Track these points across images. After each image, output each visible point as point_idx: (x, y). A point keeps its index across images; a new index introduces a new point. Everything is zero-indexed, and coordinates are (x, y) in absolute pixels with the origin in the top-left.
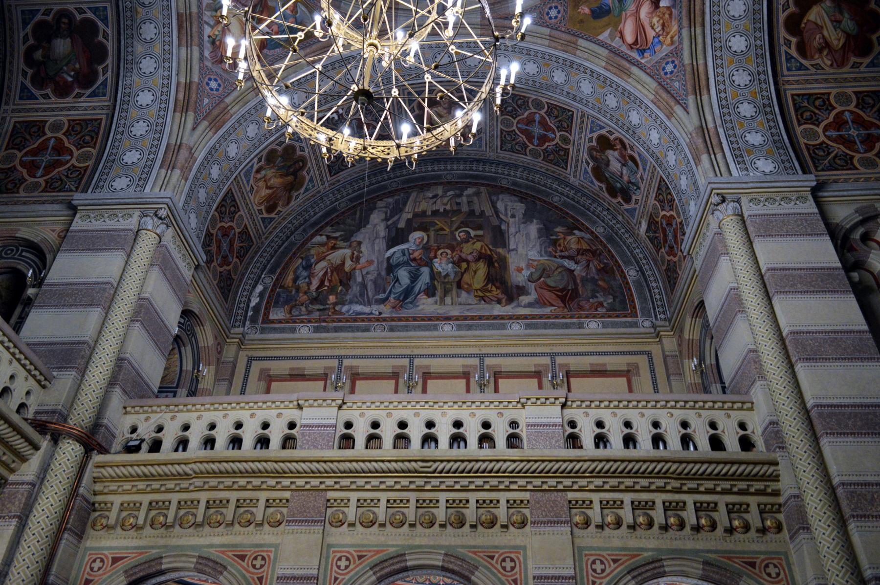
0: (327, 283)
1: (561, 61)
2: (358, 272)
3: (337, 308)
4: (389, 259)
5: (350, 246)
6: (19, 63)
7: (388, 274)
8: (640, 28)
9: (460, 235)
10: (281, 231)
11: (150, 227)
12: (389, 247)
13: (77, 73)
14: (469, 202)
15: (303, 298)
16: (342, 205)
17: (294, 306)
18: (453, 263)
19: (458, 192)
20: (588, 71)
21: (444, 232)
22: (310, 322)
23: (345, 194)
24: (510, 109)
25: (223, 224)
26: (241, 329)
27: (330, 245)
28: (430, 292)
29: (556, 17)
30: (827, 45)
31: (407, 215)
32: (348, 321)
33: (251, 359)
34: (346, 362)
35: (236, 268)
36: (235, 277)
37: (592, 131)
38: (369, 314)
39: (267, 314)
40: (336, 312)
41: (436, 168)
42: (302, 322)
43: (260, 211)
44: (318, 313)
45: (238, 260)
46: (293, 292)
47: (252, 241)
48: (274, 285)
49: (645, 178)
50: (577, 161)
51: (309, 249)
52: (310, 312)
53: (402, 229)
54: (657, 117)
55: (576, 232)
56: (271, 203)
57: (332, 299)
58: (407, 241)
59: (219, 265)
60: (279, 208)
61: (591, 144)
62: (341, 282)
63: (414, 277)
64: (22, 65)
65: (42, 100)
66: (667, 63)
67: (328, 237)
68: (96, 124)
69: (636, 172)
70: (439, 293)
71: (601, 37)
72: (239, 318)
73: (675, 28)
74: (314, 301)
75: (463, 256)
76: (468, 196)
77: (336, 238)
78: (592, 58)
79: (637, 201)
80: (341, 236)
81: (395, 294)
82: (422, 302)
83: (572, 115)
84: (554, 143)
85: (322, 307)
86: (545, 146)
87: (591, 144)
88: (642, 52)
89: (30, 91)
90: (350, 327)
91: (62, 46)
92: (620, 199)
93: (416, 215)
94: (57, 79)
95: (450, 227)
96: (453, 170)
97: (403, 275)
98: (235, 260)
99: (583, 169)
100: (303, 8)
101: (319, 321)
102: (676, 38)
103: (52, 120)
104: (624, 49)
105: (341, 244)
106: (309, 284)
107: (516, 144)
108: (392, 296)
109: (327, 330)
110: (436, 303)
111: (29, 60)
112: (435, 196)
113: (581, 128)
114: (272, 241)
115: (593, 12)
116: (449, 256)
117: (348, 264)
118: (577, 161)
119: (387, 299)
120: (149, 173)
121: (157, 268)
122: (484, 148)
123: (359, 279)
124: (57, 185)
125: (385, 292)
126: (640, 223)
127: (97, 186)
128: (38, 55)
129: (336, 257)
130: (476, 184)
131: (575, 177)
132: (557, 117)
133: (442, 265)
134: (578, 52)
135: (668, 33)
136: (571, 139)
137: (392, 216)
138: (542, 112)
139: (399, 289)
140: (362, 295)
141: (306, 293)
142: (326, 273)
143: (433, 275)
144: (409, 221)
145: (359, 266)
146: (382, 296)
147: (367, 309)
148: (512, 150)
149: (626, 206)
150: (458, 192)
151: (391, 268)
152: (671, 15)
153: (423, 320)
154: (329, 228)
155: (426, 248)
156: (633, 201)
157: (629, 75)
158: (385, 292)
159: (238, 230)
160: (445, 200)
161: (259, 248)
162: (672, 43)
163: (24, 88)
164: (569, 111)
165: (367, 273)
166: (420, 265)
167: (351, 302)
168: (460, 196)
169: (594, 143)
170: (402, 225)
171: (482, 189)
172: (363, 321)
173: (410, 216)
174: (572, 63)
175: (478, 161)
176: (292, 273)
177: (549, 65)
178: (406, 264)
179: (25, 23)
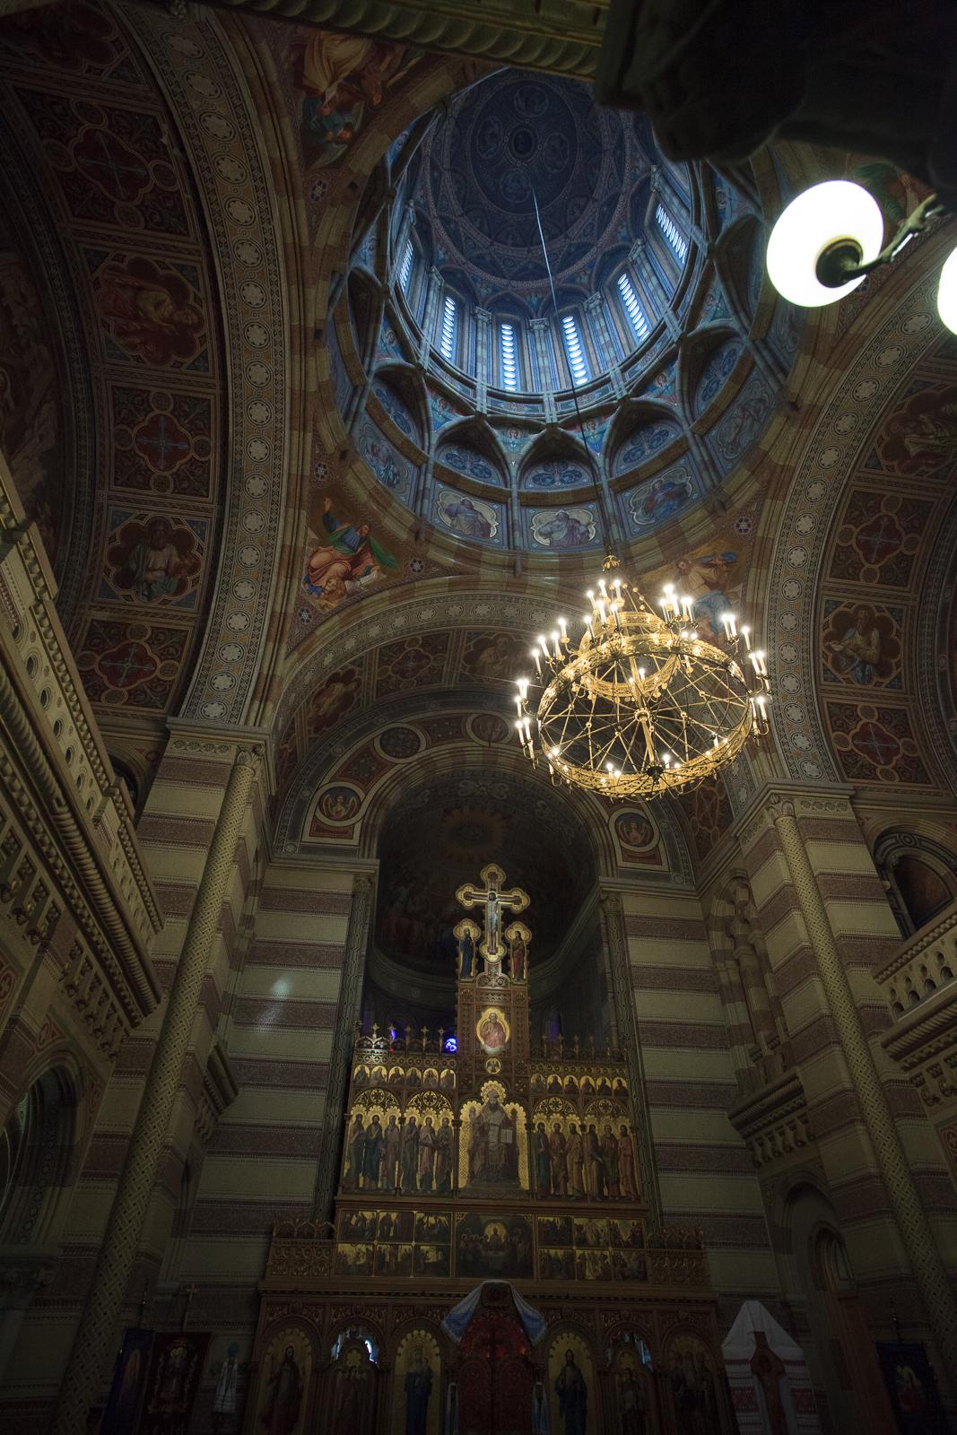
8: (325, 567)
20: (274, 524)
24: (186, 408)
30: (319, 707)
37: (191, 523)
49: (168, 607)
50: (137, 502)
54: (262, 621)
55: (52, 529)
61: (172, 522)
66: (307, 611)
69: (168, 592)
71: (310, 532)
73: (334, 605)
78: (289, 528)
79: (127, 597)
83: (202, 495)
84: (153, 469)
86: (142, 455)
87: (172, 522)
88: (308, 581)
92: (114, 571)
99: (128, 510)
100: (339, 154)
102: (328, 610)
104: (306, 559)
113: (188, 507)
115: (327, 515)
118: (137, 502)
126: (102, 609)
131: (110, 498)
132: (192, 473)
135: (327, 599)
136: (168, 493)
138: (192, 453)
149: (110, 581)
152: (342, 595)
156: (126, 592)
157: (290, 577)
162: (323, 608)
164: (207, 491)
169: (175, 527)
174: (278, 503)
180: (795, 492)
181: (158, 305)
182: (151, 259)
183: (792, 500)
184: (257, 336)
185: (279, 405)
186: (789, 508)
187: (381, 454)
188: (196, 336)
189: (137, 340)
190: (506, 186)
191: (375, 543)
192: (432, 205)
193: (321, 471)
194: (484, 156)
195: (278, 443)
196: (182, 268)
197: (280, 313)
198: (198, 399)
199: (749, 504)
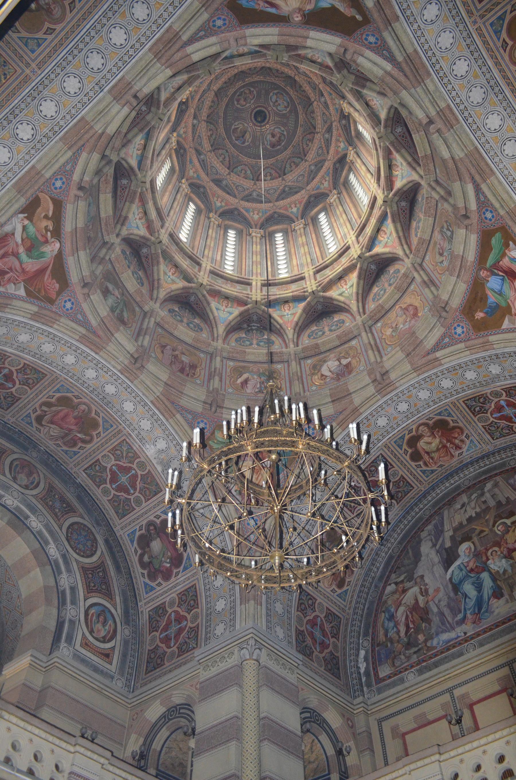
0: (411, 626)
1: (487, 359)
2: (431, 603)
3: (429, 644)
4: (451, 579)
5: (416, 583)
6: (138, 570)
7: (456, 594)
9: (499, 529)
10: (358, 596)
11: (248, 657)
12: (446, 569)
13: (171, 559)
14: (492, 496)
15: (398, 647)
16: (395, 551)
17: (395, 658)
18: (505, 557)
19: (479, 492)
21: (485, 533)
22: (412, 667)
23: (393, 540)
25: (308, 618)
26: (361, 699)
27: (400, 589)
28: (497, 594)
29: (463, 332)
31: (448, 534)
32: (442, 653)
33: (380, 722)
34: (457, 693)
35: (335, 646)
36: (338, 654)
38: (456, 639)
39: (376, 674)
40: (429, 649)
41: (452, 482)
42: (406, 670)
43: (333, 591)
44: (415, 656)
45: (334, 639)
46: (389, 645)
47: (339, 617)
48: (372, 646)
51: (386, 602)
52: (408, 658)
53: (450, 548)
56: (339, 579)
57: (421, 637)
58: (459, 556)
59: (320, 652)
60: (347, 580)
62: (422, 619)
63: (479, 587)
64: (141, 570)
65: (158, 588)
67: (396, 584)
68: (193, 589)
70: (505, 592)
72: (356, 688)
74: (409, 645)
75: (510, 546)
76: (489, 491)
77: (402, 582)
80: (405, 578)
81: (469, 609)
82: (495, 606)
85: (416, 649)
89: (150, 586)
90: (446, 657)
91: (156, 545)
93: (455, 530)
94: (162, 569)
95: (488, 526)
96: (466, 475)
97: (468, 588)
98: (332, 640)
101: (419, 663)
103: (168, 599)
105: (407, 585)
106: (398, 632)
107: (502, 429)
108: (468, 612)
109: (429, 669)
110: (507, 602)
111: (143, 565)
112: (463, 505)
114: (355, 608)
116: (499, 553)
117: (421, 600)
119: (465, 617)
120: (234, 613)
121: (265, 688)
122: (479, 446)
123: (435, 610)
124: (184, 647)
125: (460, 612)
127: (206, 639)
128: (146, 559)
129: (409, 598)
130: (490, 477)
133: (498, 564)
134: (495, 346)
137: (437, 540)
139: (471, 603)
140: (443, 624)
141: (398, 642)
142: (407, 617)
143: (494, 577)
144: (452, 538)
145: (430, 598)
146: (460, 616)
147: (452, 635)
148: (502, 436)
150: (479, 492)
151: (456, 588)
153: (504, 623)
154: (393, 576)
155: (477, 555)
158: (460, 612)
159: (322, 616)
160: (473, 504)
161: (347, 619)
163: (146, 584)
165: (439, 601)
166: (479, 573)
167: (437, 634)
168: (483, 494)
170: (448, 544)
171: (498, 478)
172: (454, 647)
173: (451, 533)
175: (482, 458)
176: (381, 629)
177: (481, 366)
178: (467, 577)
179: (132, 542)
180: (159, 26)
181: (430, 443)
182: (408, 458)
183: (165, 21)
184: (403, 407)
185: (434, 377)
186: (171, 15)
187: (442, 243)
188: (431, 422)
189: (457, 441)
190: (286, 107)
191: (490, 262)
192: (324, 169)
193: (459, 330)
194: (285, 133)
195: (458, 368)
196: (400, 447)
197: (381, 406)
198: (468, 406)
199: (201, 38)
